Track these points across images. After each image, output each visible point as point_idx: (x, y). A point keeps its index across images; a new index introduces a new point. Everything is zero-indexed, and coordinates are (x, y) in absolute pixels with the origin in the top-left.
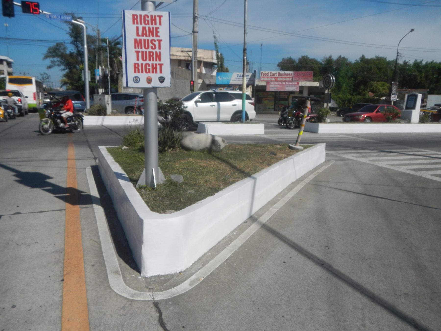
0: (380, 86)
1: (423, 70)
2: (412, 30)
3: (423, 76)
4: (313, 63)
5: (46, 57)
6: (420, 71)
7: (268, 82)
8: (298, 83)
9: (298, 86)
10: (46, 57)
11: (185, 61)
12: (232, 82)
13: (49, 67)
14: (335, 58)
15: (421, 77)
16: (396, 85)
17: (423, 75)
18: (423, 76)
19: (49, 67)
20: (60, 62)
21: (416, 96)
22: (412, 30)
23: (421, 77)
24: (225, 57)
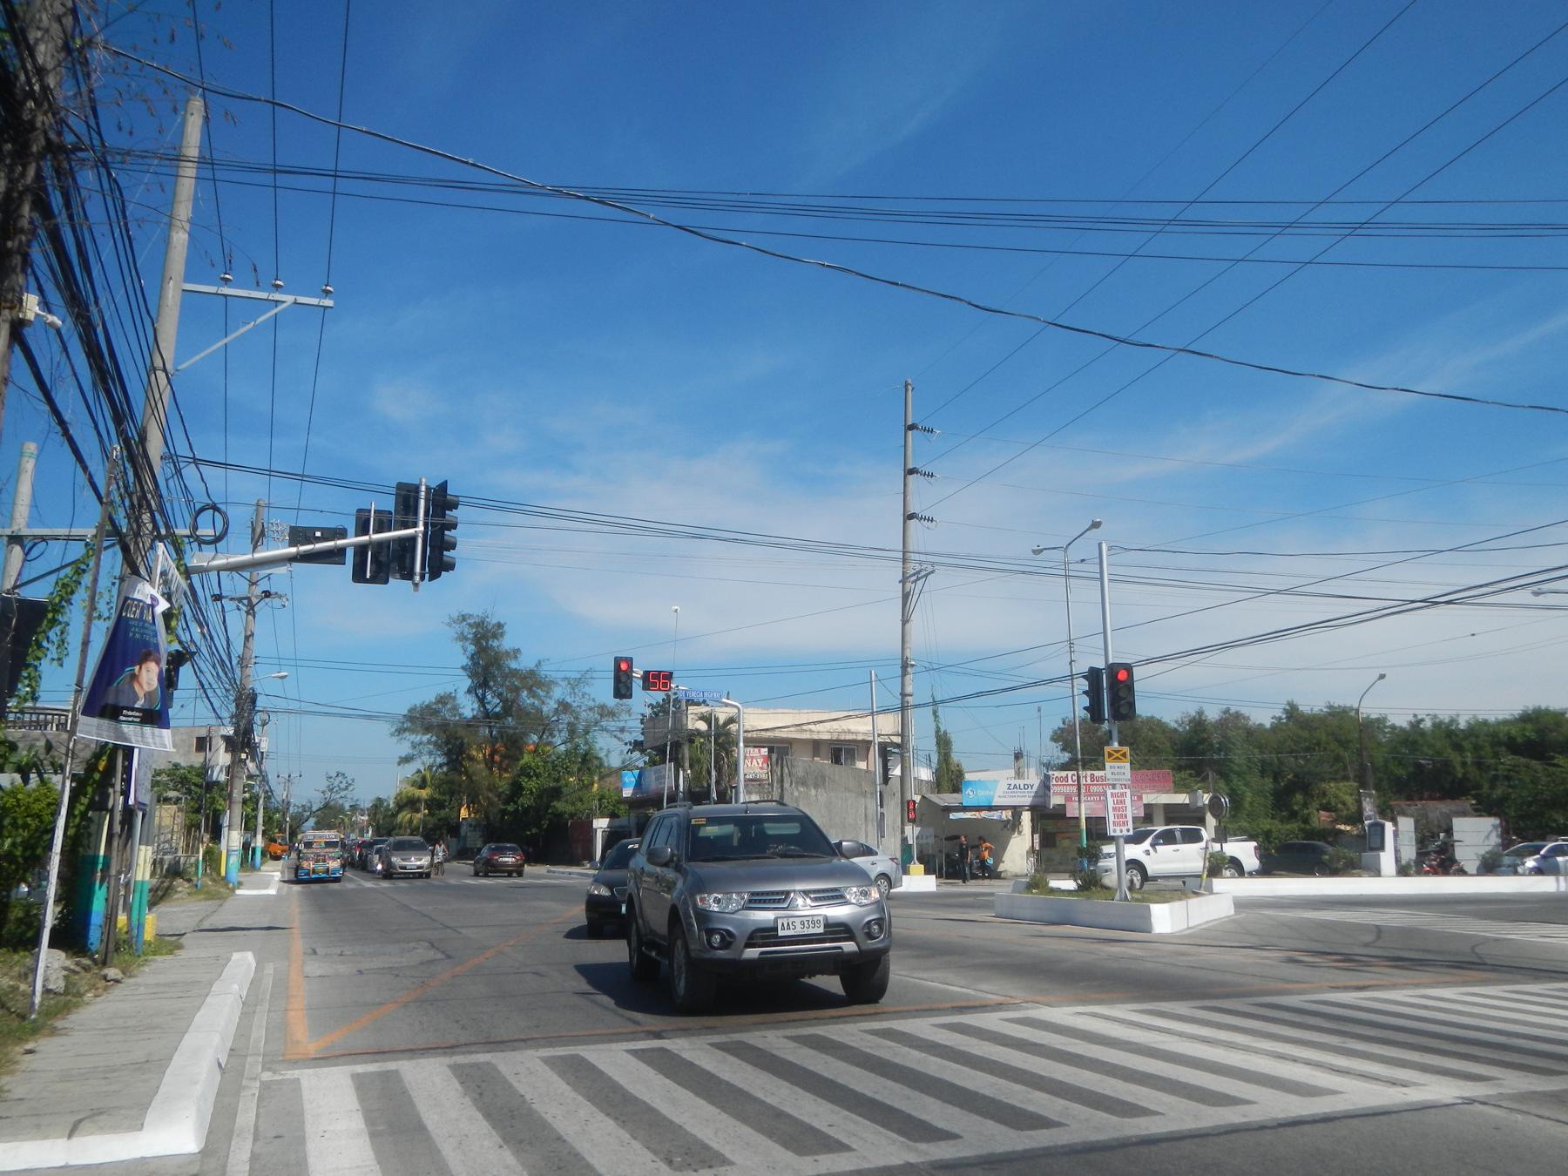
0: (1341, 791)
1: (1466, 744)
2: (1382, 677)
3: (1469, 760)
4: (1151, 729)
5: (400, 731)
6: (1458, 747)
7: (1068, 798)
8: (1140, 798)
9: (1140, 804)
10: (400, 731)
11: (830, 742)
12: (996, 802)
13: (406, 760)
14: (1212, 714)
15: (1464, 764)
16: (1370, 796)
17: (1469, 758)
18: (1469, 760)
19: (406, 760)
20: (435, 744)
21: (1383, 827)
22: (1382, 677)
23: (1464, 764)
24: (953, 737)
